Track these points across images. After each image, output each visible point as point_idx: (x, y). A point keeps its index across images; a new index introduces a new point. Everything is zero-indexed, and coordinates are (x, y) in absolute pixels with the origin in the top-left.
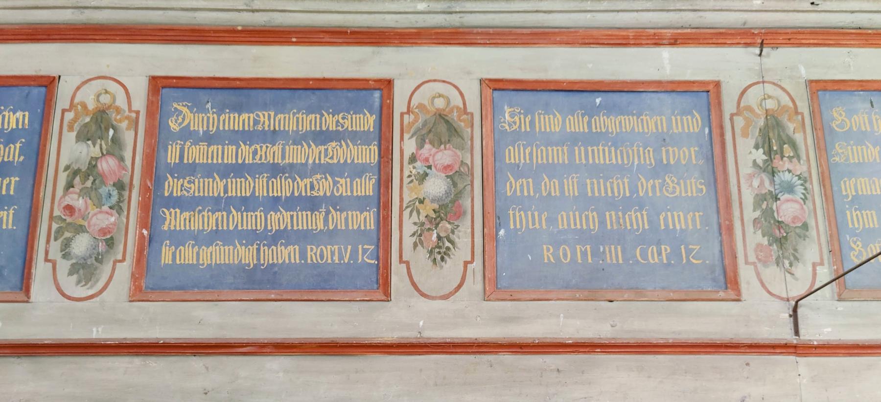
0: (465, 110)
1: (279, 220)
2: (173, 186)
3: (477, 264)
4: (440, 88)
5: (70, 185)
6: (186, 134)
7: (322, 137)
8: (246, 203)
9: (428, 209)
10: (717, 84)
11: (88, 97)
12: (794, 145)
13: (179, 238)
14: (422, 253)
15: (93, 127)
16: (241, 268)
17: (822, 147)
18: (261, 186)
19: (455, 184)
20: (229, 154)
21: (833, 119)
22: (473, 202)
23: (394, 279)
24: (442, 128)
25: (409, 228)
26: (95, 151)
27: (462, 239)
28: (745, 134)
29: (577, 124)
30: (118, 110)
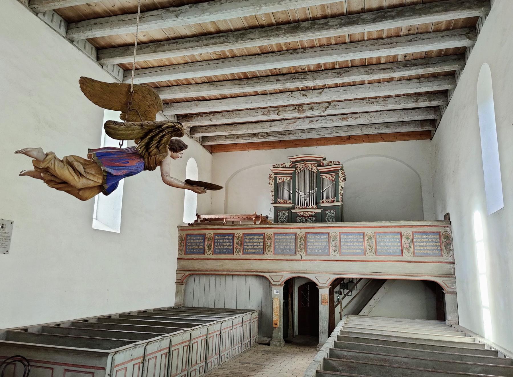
1: (255, 247)
6: (246, 239)
7: (258, 239)
8: (252, 246)
9: (268, 246)
17: (306, 240)
20: (250, 241)
22: (272, 246)
27: (271, 249)
29: (282, 237)
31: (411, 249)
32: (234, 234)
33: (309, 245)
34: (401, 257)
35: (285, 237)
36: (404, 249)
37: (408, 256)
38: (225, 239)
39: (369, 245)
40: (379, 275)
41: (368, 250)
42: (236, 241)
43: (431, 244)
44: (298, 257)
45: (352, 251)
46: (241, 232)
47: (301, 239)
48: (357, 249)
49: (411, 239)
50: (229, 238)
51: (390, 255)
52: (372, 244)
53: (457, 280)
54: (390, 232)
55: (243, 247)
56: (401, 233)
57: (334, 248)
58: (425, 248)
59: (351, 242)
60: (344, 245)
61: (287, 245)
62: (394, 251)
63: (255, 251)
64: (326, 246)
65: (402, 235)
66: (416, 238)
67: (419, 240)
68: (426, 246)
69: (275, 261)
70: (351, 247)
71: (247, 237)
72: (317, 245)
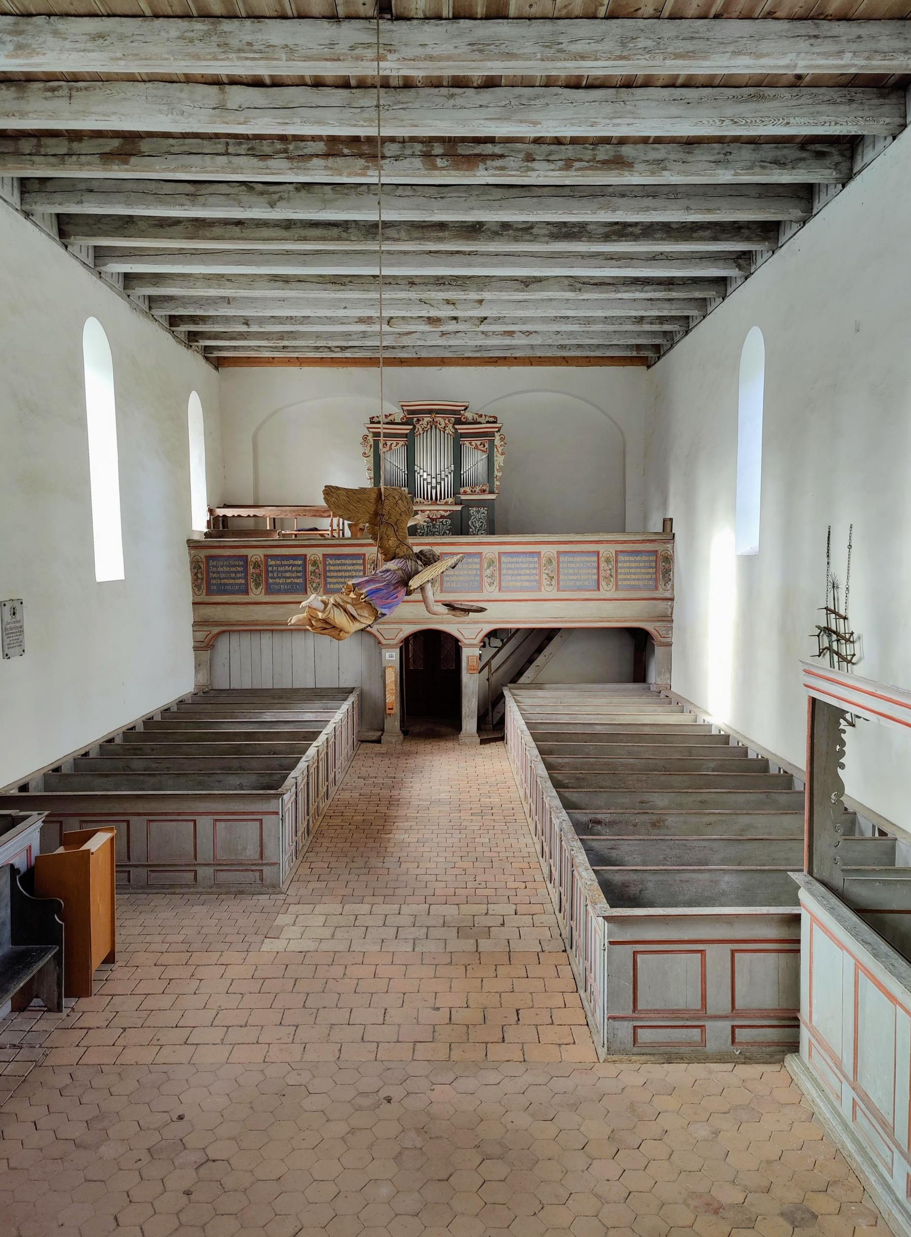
7: (353, 565)
11: (312, 558)
13: (330, 583)
20: (337, 568)
31: (612, 579)
32: (305, 556)
36: (601, 578)
37: (607, 591)
38: (289, 566)
41: (545, 582)
42: (310, 568)
43: (643, 571)
45: (519, 584)
46: (319, 553)
48: (527, 581)
49: (613, 563)
51: (580, 589)
55: (325, 580)
56: (598, 553)
57: (489, 580)
58: (633, 577)
59: (518, 569)
62: (587, 583)
64: (476, 575)
65: (600, 556)
66: (621, 562)
68: (635, 574)
71: (331, 562)
72: (460, 575)
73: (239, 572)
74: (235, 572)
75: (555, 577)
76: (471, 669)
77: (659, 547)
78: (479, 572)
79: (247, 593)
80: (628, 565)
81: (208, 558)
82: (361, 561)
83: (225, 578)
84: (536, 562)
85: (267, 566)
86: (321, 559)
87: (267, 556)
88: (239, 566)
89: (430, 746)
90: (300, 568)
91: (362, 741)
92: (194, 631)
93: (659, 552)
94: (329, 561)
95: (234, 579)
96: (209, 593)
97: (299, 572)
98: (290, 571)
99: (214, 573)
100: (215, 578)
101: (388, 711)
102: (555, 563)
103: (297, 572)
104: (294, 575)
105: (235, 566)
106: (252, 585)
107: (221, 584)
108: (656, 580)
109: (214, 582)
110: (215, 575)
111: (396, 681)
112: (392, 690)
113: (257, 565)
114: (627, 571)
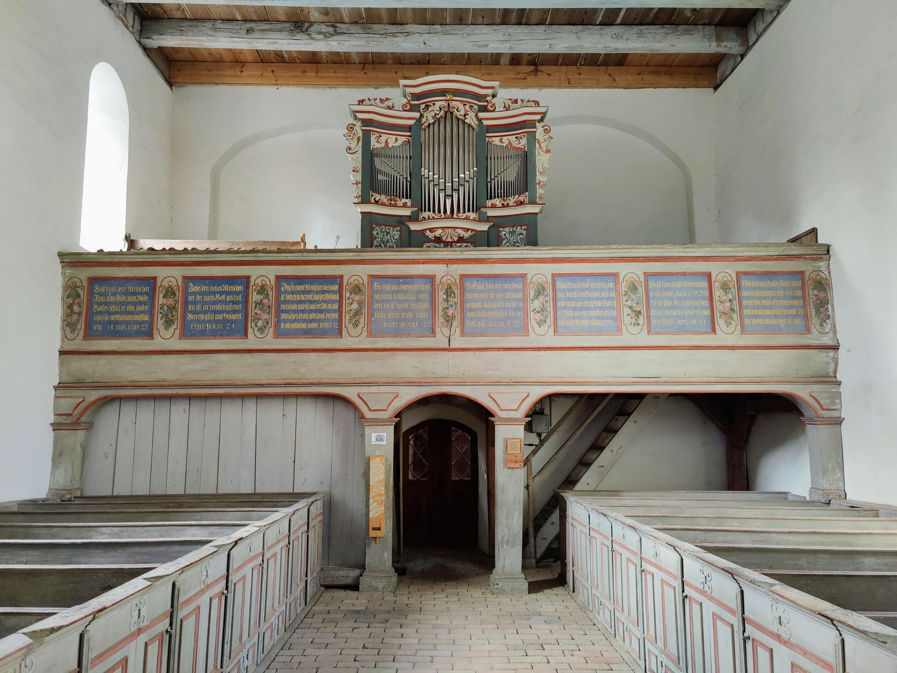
0: (363, 284)
1: (312, 316)
2: (283, 307)
3: (366, 328)
4: (356, 277)
5: (256, 307)
6: (286, 292)
7: (324, 292)
8: (303, 311)
9: (352, 313)
10: (435, 276)
11: (259, 281)
12: (454, 294)
13: (285, 321)
14: (351, 325)
15: (261, 291)
16: (303, 329)
17: (462, 294)
18: (307, 306)
19: (360, 306)
21: (467, 286)
22: (365, 311)
23: (343, 332)
24: (357, 289)
25: (347, 318)
26: (262, 297)
27: (362, 321)
28: (441, 291)
29: (395, 288)
30: (267, 286)
31: (735, 316)
33: (471, 310)
34: (711, 336)
35: (404, 287)
36: (717, 315)
37: (727, 334)
38: (221, 293)
39: (630, 308)
40: (658, 383)
42: (255, 297)
44: (440, 341)
45: (585, 323)
46: (271, 272)
47: (449, 292)
48: (598, 318)
49: (735, 291)
50: (233, 289)
51: (683, 331)
52: (638, 303)
53: (842, 389)
54: (684, 274)
55: (277, 316)
57: (538, 316)
59: (583, 299)
60: (564, 308)
61: (409, 310)
62: (694, 322)
63: (314, 325)
64: (517, 309)
65: (713, 279)
66: (747, 289)
67: (753, 293)
68: (770, 307)
69: (373, 353)
70: (584, 313)
72: (492, 309)
73: (141, 303)
74: (135, 304)
75: (643, 311)
76: (509, 462)
77: (807, 267)
78: (521, 305)
79: (150, 335)
80: (758, 293)
81: (92, 280)
82: (336, 288)
83: (117, 313)
84: (610, 289)
85: (186, 293)
86: (273, 283)
87: (186, 279)
88: (141, 294)
89: (443, 596)
90: (239, 298)
91: (328, 587)
92: (56, 397)
93: (807, 274)
94: (286, 287)
95: (132, 313)
96: (89, 335)
97: (237, 303)
98: (222, 302)
99: (100, 304)
100: (101, 313)
101: (372, 533)
102: (641, 290)
103: (234, 303)
104: (229, 307)
105: (135, 294)
106: (160, 323)
107: (110, 322)
108: (806, 317)
109: (99, 318)
110: (102, 308)
111: (387, 480)
112: (380, 495)
113: (170, 292)
114: (757, 303)
